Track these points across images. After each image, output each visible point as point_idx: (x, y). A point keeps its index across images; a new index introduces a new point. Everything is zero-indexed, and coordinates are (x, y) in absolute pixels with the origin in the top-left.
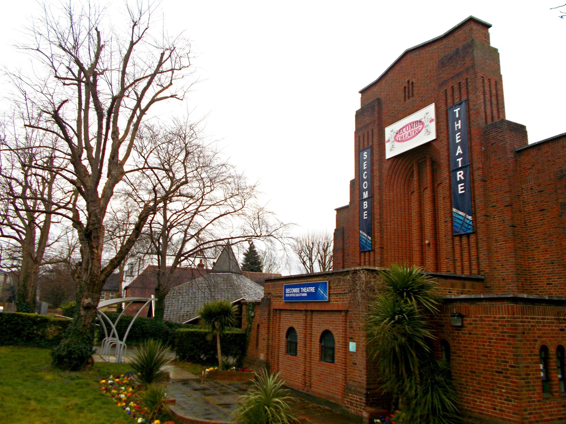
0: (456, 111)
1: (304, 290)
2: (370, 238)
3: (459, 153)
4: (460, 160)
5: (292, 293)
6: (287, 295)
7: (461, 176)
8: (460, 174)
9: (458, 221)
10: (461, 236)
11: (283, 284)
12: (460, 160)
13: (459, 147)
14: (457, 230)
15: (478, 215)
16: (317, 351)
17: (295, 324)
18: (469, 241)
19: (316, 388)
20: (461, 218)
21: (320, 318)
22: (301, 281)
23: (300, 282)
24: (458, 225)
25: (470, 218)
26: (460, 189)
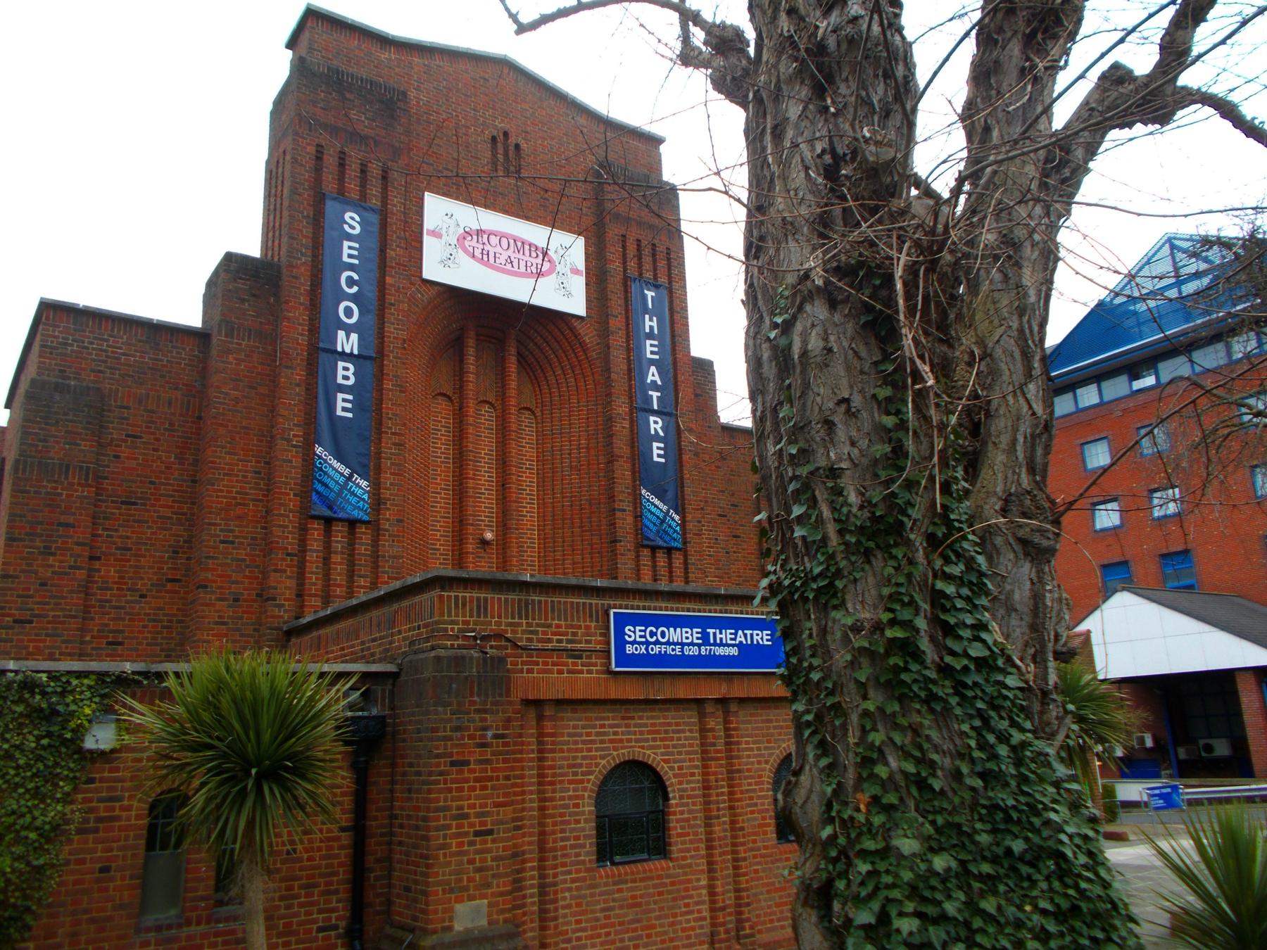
0: (650, 294)
1: (726, 635)
2: (364, 484)
3: (654, 382)
4: (655, 395)
5: (657, 642)
6: (629, 649)
7: (658, 427)
8: (656, 422)
9: (650, 516)
10: (654, 549)
11: (610, 607)
12: (655, 395)
13: (653, 369)
14: (651, 536)
15: (689, 517)
16: (764, 818)
17: (651, 747)
18: (670, 564)
19: (768, 930)
20: (658, 512)
21: (770, 721)
22: (688, 605)
23: (688, 610)
24: (651, 526)
25: (677, 518)
26: (657, 450)
